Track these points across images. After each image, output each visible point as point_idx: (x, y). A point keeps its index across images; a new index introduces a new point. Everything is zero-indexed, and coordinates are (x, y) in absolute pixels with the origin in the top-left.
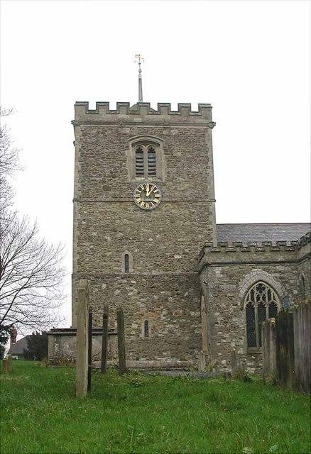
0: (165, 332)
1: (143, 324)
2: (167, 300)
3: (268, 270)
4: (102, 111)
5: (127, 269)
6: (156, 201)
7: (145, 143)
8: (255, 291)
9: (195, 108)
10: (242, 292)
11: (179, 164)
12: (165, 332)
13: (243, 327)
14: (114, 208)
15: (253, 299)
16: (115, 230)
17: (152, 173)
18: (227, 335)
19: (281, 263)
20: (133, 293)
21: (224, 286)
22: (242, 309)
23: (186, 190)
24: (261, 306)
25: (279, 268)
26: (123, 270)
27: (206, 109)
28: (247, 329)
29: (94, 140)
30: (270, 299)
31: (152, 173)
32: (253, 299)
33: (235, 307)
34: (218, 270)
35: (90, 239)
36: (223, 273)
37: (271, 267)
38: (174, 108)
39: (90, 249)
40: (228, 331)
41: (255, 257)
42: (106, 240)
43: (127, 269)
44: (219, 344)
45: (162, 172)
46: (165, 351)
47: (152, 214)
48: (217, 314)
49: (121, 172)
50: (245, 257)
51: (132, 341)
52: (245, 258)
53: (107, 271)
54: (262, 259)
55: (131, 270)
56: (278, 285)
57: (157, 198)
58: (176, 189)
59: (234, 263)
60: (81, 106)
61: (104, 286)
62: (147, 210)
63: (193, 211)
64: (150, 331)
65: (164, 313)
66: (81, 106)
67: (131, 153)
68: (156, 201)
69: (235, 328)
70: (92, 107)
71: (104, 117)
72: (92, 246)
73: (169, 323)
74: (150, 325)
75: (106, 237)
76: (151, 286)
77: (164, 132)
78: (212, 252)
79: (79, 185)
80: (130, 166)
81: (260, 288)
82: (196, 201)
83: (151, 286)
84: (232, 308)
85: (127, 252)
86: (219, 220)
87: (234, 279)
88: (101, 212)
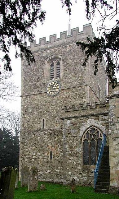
0: (60, 157)
1: (50, 153)
3: (98, 119)
6: (57, 90)
8: (89, 132)
10: (81, 133)
12: (60, 157)
13: (81, 153)
14: (39, 97)
15: (88, 137)
16: (38, 108)
18: (72, 158)
20: (45, 138)
21: (71, 131)
22: (81, 143)
23: (73, 82)
26: (42, 127)
28: (83, 154)
30: (98, 136)
31: (59, 76)
32: (88, 137)
33: (77, 142)
34: (68, 122)
35: (28, 114)
36: (71, 123)
37: (100, 117)
39: (28, 119)
40: (72, 155)
41: (90, 112)
42: (35, 114)
44: (67, 163)
46: (59, 166)
47: (56, 98)
48: (67, 146)
49: (42, 78)
50: (84, 113)
51: (45, 162)
52: (84, 113)
53: (35, 129)
54: (94, 112)
55: (45, 127)
56: (103, 128)
57: (58, 89)
58: (68, 82)
59: (77, 117)
61: (33, 136)
63: (76, 92)
64: (53, 157)
65: (59, 147)
68: (57, 90)
69: (76, 154)
72: (29, 117)
73: (62, 152)
74: (53, 153)
75: (34, 112)
78: (65, 112)
79: (23, 88)
80: (47, 74)
82: (78, 87)
84: (75, 142)
85: (43, 118)
87: (77, 126)
88: (33, 100)
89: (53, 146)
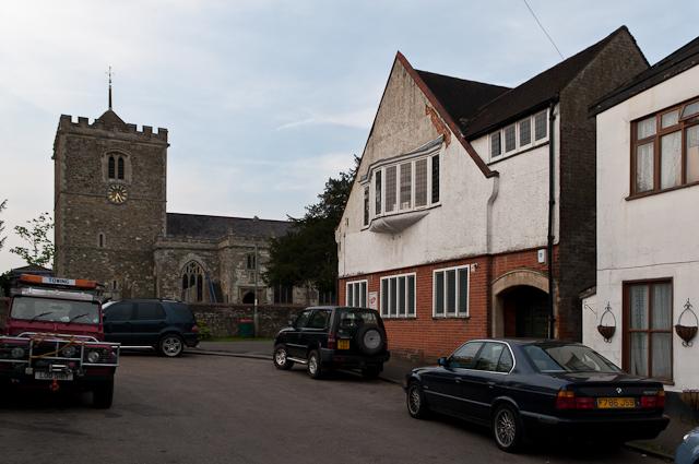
2: (129, 267)
4: (83, 125)
5: (101, 244)
7: (117, 153)
9: (155, 131)
10: (181, 266)
11: (142, 173)
14: (93, 200)
17: (121, 177)
19: (208, 250)
24: (193, 277)
25: (206, 253)
27: (163, 133)
29: (77, 147)
34: (166, 252)
35: (74, 221)
38: (140, 129)
43: (101, 244)
45: (128, 176)
55: (104, 246)
56: (204, 264)
60: (65, 119)
62: (117, 204)
66: (65, 119)
67: (105, 160)
69: (175, 289)
70: (75, 120)
71: (83, 130)
76: (118, 257)
77: (133, 147)
80: (104, 170)
81: (193, 265)
83: (118, 257)
86: (168, 211)
89: (117, 273)
